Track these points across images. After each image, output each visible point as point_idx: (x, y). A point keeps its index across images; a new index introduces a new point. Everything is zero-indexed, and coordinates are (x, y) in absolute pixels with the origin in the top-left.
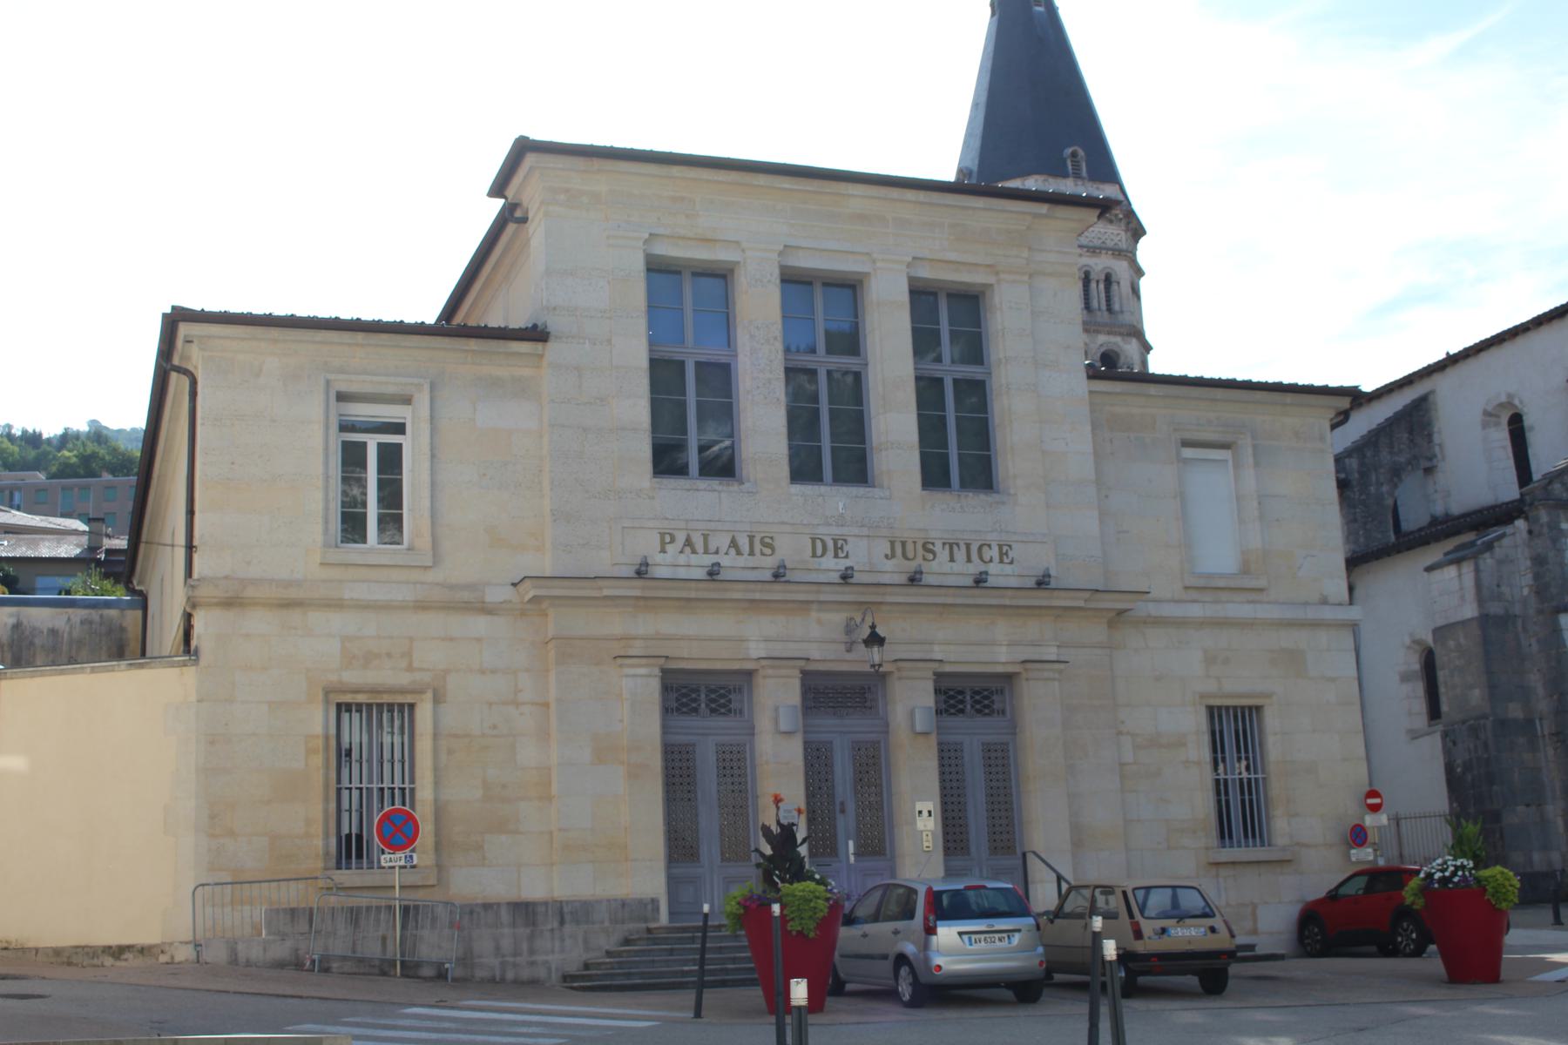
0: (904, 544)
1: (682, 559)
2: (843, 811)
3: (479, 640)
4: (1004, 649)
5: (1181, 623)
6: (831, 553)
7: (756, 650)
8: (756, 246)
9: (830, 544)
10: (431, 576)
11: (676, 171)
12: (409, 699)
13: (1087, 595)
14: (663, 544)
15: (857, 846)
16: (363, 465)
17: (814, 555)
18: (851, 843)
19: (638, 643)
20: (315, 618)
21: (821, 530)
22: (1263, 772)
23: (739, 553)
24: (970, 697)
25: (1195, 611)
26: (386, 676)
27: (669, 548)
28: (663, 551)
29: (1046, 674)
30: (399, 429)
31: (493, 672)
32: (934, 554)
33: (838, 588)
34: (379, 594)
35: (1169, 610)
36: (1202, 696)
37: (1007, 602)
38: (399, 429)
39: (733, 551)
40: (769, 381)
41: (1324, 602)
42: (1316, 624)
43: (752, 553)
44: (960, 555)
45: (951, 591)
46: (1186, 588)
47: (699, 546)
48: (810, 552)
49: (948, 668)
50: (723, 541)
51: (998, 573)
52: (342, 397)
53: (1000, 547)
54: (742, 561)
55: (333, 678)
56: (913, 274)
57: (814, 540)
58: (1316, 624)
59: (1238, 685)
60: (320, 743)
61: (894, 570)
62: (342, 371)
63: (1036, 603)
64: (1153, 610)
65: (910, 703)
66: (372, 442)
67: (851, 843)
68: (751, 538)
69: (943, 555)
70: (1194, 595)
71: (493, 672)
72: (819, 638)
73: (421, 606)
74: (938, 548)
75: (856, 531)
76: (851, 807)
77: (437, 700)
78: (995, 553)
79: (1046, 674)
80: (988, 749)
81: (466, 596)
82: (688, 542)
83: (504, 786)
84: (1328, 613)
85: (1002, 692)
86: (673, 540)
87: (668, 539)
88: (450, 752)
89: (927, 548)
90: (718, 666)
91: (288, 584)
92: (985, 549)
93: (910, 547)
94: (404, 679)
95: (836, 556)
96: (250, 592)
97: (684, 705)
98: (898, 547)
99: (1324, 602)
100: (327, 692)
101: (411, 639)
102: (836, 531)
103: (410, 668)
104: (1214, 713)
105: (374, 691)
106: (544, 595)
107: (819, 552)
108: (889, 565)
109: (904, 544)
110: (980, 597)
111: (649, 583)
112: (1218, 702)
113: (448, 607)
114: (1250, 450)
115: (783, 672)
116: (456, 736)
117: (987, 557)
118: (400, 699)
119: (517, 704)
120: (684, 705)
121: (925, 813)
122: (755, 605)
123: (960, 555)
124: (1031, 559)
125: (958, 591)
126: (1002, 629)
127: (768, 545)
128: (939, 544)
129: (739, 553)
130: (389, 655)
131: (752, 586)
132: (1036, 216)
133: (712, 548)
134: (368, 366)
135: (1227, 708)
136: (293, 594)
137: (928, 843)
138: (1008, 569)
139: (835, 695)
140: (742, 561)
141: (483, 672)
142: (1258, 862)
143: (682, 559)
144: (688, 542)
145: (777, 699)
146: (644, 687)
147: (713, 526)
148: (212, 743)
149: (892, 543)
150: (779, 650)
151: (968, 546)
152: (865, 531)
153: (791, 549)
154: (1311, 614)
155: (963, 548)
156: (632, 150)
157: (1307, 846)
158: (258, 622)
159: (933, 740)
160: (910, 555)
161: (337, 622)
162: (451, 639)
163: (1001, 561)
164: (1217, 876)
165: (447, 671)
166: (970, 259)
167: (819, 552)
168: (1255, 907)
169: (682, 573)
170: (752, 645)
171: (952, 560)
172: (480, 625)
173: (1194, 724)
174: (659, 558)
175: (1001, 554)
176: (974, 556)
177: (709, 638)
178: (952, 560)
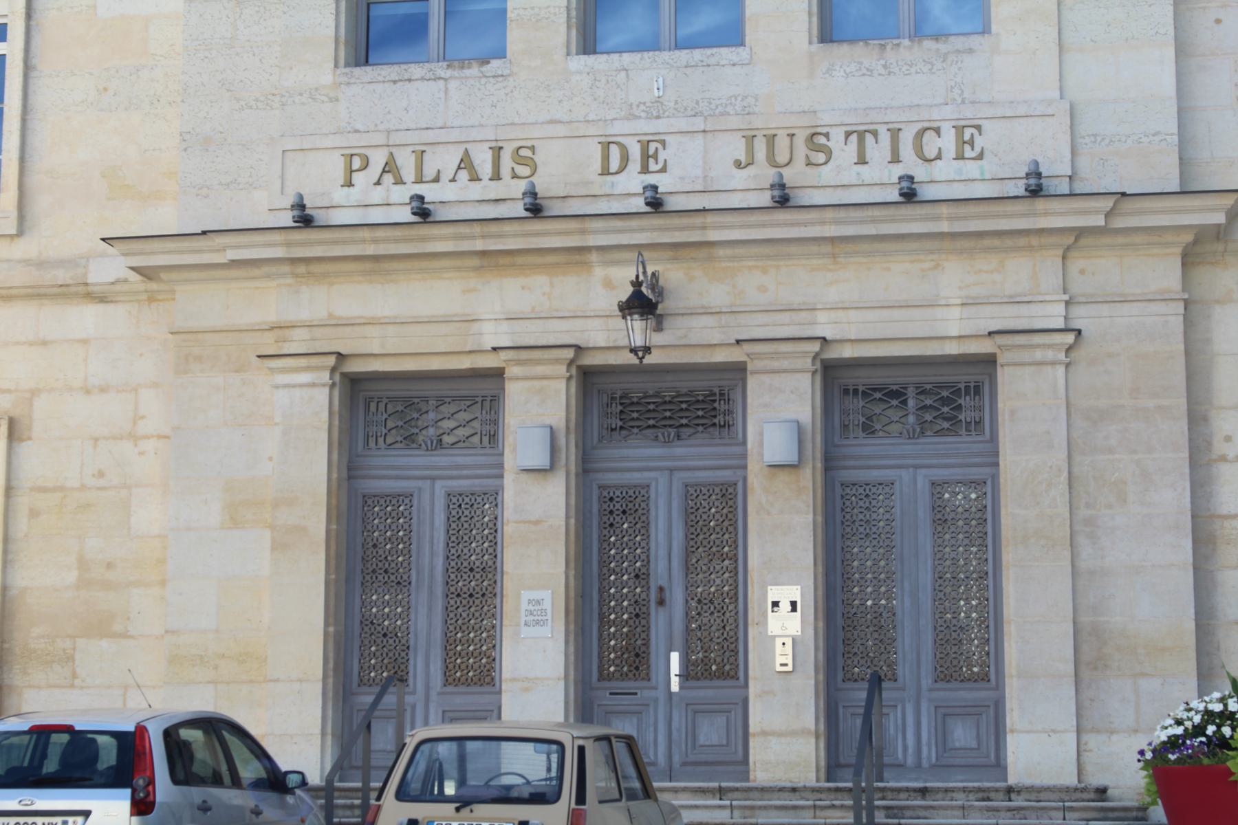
0: (771, 140)
1: (377, 195)
2: (661, 602)
3: (85, 342)
4: (956, 312)
6: (635, 164)
7: (495, 334)
13: (1108, 203)
15: (686, 663)
17: (606, 172)
18: (675, 657)
21: (618, 128)
23: (475, 178)
27: (358, 178)
28: (350, 184)
29: (1038, 355)
32: (829, 153)
37: (945, 227)
39: (464, 175)
43: (496, 176)
44: (878, 151)
45: (830, 214)
47: (408, 173)
48: (597, 166)
49: (848, 352)
50: (447, 160)
51: (944, 176)
53: (960, 130)
54: (475, 191)
57: (606, 146)
61: (750, 186)
65: (778, 414)
68: (497, 151)
69: (845, 152)
71: (103, 390)
75: (682, 124)
76: (677, 596)
78: (948, 142)
79: (1038, 355)
81: (62, 276)
82: (390, 167)
83: (109, 566)
85: (978, 390)
86: (365, 166)
87: (357, 163)
88: (34, 513)
89: (816, 141)
90: (435, 364)
92: (929, 135)
93: (782, 144)
95: (645, 170)
97: (945, 401)
98: (760, 142)
102: (646, 127)
106: (159, 265)
107: (614, 166)
108: (741, 178)
109: (771, 140)
110: (912, 222)
113: (37, 294)
115: (540, 370)
116: (43, 490)
117: (930, 152)
119: (134, 438)
120: (945, 401)
121: (785, 606)
123: (878, 151)
125: (842, 214)
126: (954, 277)
127: (526, 158)
128: (837, 136)
133: (429, 173)
137: (783, 656)
138: (971, 169)
139: (650, 406)
140: (475, 191)
143: (377, 195)
144: (390, 167)
145: (537, 410)
146: (308, 404)
147: (430, 136)
149: (750, 140)
150: (533, 333)
151: (895, 134)
152: (699, 124)
153: (563, 170)
155: (885, 137)
159: (809, 479)
160: (782, 158)
162: (44, 343)
163: (960, 157)
165: (35, 392)
167: (614, 166)
169: (377, 216)
170: (487, 327)
171: (862, 161)
172: (85, 319)
174: (340, 195)
175: (961, 143)
177: (415, 319)
178: (862, 161)
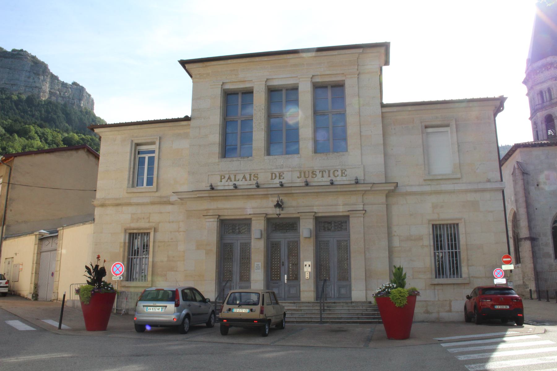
0: (305, 173)
1: (227, 184)
2: (283, 265)
3: (169, 213)
4: (341, 207)
5: (422, 193)
6: (278, 178)
7: (250, 211)
8: (257, 79)
9: (278, 175)
10: (157, 194)
11: (229, 61)
12: (148, 231)
13: (371, 185)
14: (221, 179)
15: (288, 277)
16: (144, 164)
17: (272, 179)
18: (286, 276)
19: (211, 211)
20: (125, 208)
21: (275, 170)
22: (459, 249)
23: (246, 180)
24: (324, 224)
25: (427, 188)
26: (143, 225)
27: (223, 180)
28: (221, 181)
29: (358, 215)
30: (153, 152)
31: (173, 222)
32: (316, 175)
33: (279, 189)
34: (140, 200)
35: (415, 189)
36: (429, 221)
37: (339, 190)
38: (153, 152)
39: (244, 180)
40: (260, 123)
41: (489, 181)
42: (484, 190)
43: (250, 180)
44: (326, 175)
45: (316, 187)
46: (425, 180)
47: (233, 179)
48: (270, 178)
49: (320, 215)
50: (240, 177)
51: (339, 180)
52: (138, 145)
53: (342, 171)
54: (246, 183)
55: (128, 225)
56: (314, 80)
57: (272, 174)
58: (484, 190)
59: (447, 215)
60: (122, 245)
61: (300, 182)
62: (137, 137)
63: (306, 191)
64: (409, 189)
65: (306, 227)
66: (147, 156)
67: (286, 276)
68: (250, 175)
69: (319, 175)
70: (429, 182)
71: (173, 222)
72: (267, 206)
73: (153, 203)
74: (318, 173)
75: (287, 169)
76: (286, 263)
77: (155, 231)
78: (339, 173)
79: (358, 215)
80: (339, 242)
81: (165, 199)
82: (229, 178)
83: (173, 257)
84: (489, 186)
85: (346, 222)
86: (224, 178)
87: (223, 177)
88: (159, 247)
89: (314, 173)
90: (238, 217)
91: (116, 199)
92: (336, 172)
93: (307, 173)
94: (147, 225)
95: (280, 178)
96: (107, 202)
97: (340, 224)
98: (303, 173)
99: (489, 181)
100: (125, 230)
101: (150, 213)
102: (281, 170)
103: (149, 222)
104: (435, 227)
105: (137, 229)
106: (183, 198)
107: (274, 178)
108: (299, 180)
109: (305, 173)
110: (332, 189)
111: (285, 189)
112: (437, 223)
113: (160, 203)
114: (455, 126)
115: (258, 218)
116: (161, 242)
117: (336, 175)
118: (146, 231)
119: (179, 232)
120: (340, 224)
121: (308, 266)
122: (249, 197)
123: (326, 175)
124: (353, 174)
125: (319, 187)
126: (341, 200)
127: (256, 176)
128: (318, 172)
129: (246, 180)
130: (144, 218)
131: (244, 190)
132: (360, 54)
133: (237, 179)
134: (141, 135)
135: (443, 225)
136: (118, 202)
137: (307, 276)
138: (344, 178)
139: (281, 225)
140: (246, 183)
141: (169, 222)
142: (454, 284)
143: (227, 184)
144: (229, 178)
145: (258, 226)
146: (212, 225)
147: (238, 172)
148: (96, 245)
149: (300, 173)
150: (258, 211)
151: (329, 171)
152: (290, 169)
153: (263, 178)
154: (481, 186)
155: (327, 172)
156: (202, 59)
157: (475, 277)
158: (110, 210)
159: (312, 240)
160: (307, 176)
161: (130, 209)
162: (161, 213)
163: (342, 176)
164: (435, 289)
165: (159, 222)
166: (335, 72)
167: (274, 178)
168: (450, 301)
169: (227, 188)
170: (248, 210)
171: (323, 177)
172: (169, 208)
173: (426, 232)
174: (219, 184)
175: (342, 173)
176: (331, 175)
177: (234, 208)
178: (323, 177)
